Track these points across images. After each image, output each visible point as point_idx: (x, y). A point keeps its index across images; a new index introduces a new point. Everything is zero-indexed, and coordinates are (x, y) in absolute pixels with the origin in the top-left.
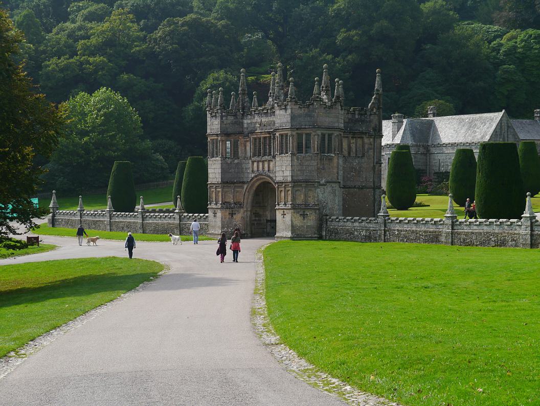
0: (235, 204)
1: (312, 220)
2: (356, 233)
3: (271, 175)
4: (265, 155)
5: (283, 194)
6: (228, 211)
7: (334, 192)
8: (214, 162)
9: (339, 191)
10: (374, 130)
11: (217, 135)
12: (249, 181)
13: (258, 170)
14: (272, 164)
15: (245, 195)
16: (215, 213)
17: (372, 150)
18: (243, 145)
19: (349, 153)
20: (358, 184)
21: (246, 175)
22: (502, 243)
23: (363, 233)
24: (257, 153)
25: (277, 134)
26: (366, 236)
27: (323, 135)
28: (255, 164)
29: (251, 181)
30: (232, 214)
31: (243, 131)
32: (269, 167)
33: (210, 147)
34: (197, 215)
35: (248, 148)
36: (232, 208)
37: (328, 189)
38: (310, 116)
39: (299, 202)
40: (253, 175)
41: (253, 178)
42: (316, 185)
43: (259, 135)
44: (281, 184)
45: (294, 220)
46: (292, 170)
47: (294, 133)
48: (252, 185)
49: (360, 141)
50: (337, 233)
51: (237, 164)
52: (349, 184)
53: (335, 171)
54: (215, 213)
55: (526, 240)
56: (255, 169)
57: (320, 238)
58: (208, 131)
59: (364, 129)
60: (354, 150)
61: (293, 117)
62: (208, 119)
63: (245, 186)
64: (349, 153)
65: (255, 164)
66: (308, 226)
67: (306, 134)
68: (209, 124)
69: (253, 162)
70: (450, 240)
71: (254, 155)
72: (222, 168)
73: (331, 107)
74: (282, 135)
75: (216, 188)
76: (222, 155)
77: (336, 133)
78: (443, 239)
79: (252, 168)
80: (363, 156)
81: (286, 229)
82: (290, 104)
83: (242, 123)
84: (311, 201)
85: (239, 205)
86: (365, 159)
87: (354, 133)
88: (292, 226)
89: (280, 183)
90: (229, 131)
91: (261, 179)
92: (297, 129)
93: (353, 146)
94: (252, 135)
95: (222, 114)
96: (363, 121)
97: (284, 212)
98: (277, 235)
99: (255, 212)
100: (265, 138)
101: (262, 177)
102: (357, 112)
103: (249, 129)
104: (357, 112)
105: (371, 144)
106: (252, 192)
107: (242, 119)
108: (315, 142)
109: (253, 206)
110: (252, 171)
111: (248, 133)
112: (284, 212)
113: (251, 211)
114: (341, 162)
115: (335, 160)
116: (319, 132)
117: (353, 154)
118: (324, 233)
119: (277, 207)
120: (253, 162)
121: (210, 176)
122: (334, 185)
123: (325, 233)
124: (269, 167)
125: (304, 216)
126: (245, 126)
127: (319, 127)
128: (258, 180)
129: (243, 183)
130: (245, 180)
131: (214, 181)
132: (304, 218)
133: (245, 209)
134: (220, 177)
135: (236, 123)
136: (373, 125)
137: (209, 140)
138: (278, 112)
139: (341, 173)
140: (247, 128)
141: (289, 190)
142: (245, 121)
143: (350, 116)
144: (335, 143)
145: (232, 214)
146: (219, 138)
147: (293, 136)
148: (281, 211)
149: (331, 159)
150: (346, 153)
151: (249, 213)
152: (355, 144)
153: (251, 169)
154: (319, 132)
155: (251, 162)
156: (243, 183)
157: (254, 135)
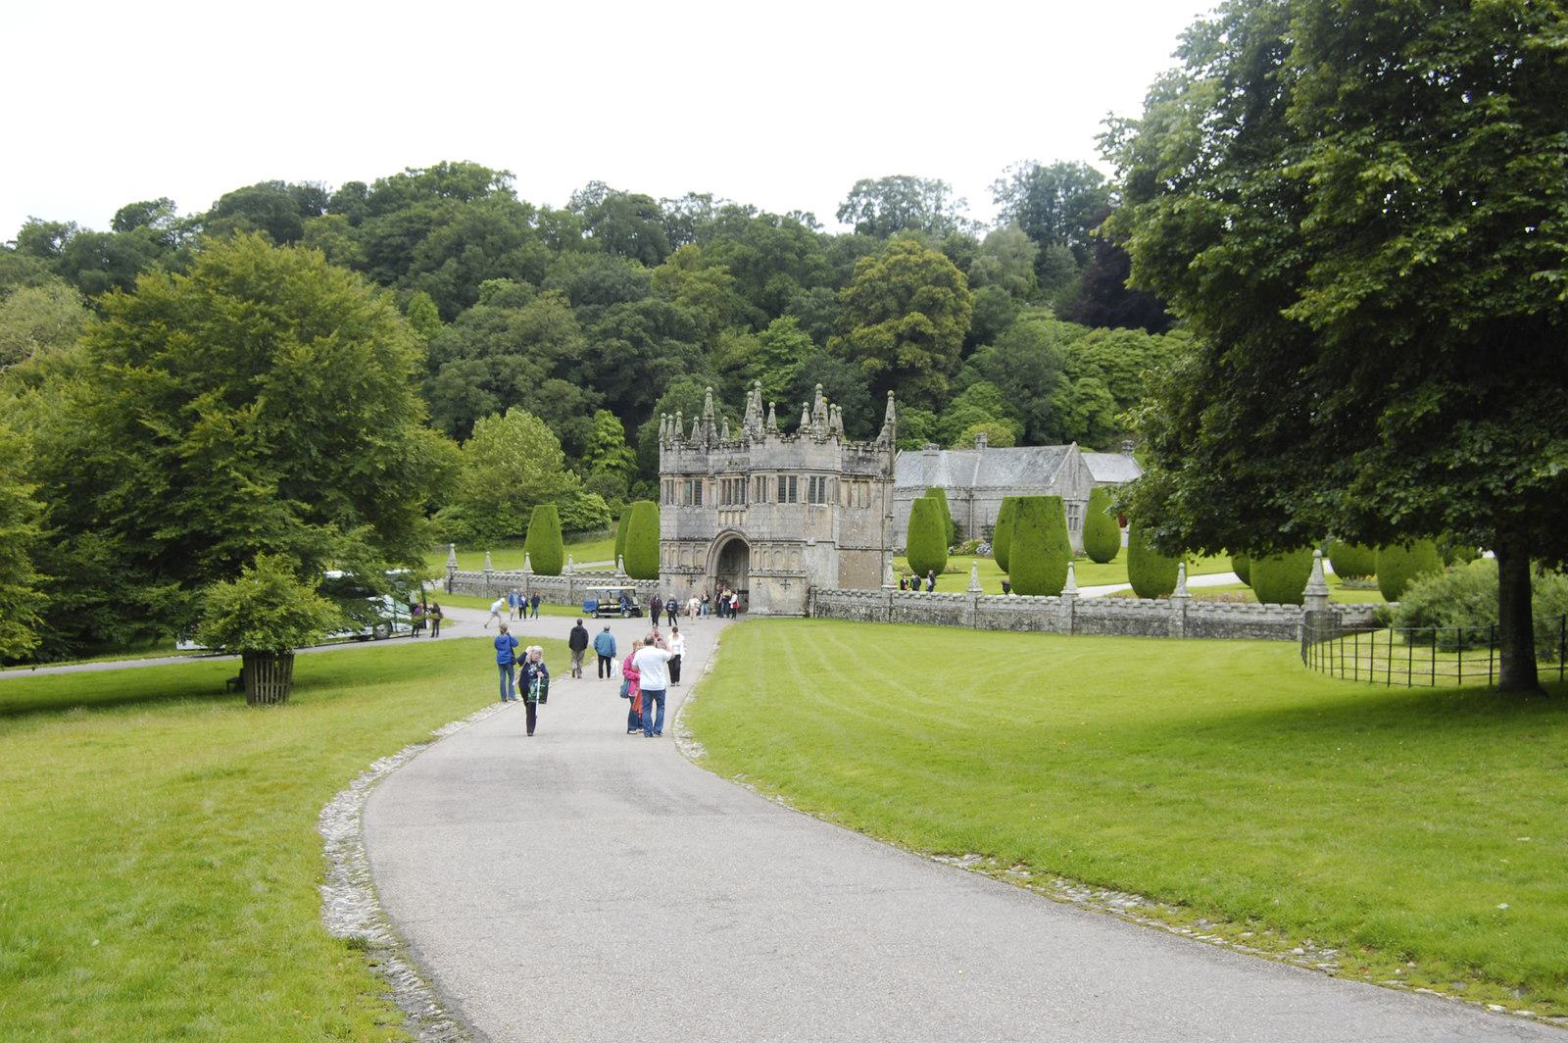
0: (695, 568)
1: (796, 592)
3: (744, 531)
4: (736, 503)
5: (758, 556)
6: (686, 578)
7: (826, 556)
9: (835, 556)
10: (884, 472)
11: (673, 475)
14: (744, 515)
15: (706, 558)
17: (880, 500)
19: (849, 503)
20: (861, 544)
22: (1035, 627)
23: (863, 611)
24: (726, 500)
25: (752, 476)
27: (813, 479)
32: (741, 520)
35: (714, 493)
37: (819, 550)
38: (796, 454)
39: (779, 567)
40: (720, 531)
42: (802, 545)
45: (772, 591)
48: (719, 543)
49: (864, 487)
51: (698, 515)
52: (848, 544)
53: (828, 527)
55: (1066, 624)
56: (723, 521)
57: (807, 615)
58: (662, 469)
59: (869, 471)
60: (856, 499)
62: (662, 453)
63: (709, 544)
64: (849, 503)
66: (790, 600)
67: (790, 477)
68: (662, 459)
69: (720, 512)
70: (973, 622)
73: (823, 442)
77: (830, 477)
78: (963, 620)
79: (718, 521)
80: (869, 506)
82: (768, 436)
83: (707, 460)
84: (795, 568)
86: (870, 512)
87: (856, 477)
90: (689, 470)
92: (778, 470)
93: (855, 494)
96: (869, 460)
98: (750, 610)
100: (737, 481)
102: (860, 448)
103: (716, 468)
104: (860, 448)
105: (879, 491)
106: (718, 552)
107: (707, 454)
108: (803, 487)
109: (719, 571)
113: (717, 578)
114: (836, 514)
115: (829, 513)
116: (808, 476)
117: (854, 504)
118: (811, 611)
119: (750, 574)
121: (663, 530)
122: (825, 545)
124: (741, 520)
125: (785, 586)
126: (711, 463)
127: (809, 470)
128: (726, 537)
129: (706, 540)
130: (709, 536)
131: (669, 537)
135: (697, 459)
136: (882, 466)
138: (753, 447)
139: (837, 530)
142: (711, 457)
143: (851, 453)
144: (829, 489)
148: (755, 580)
149: (822, 511)
150: (844, 502)
151: (714, 581)
152: (858, 490)
154: (808, 476)
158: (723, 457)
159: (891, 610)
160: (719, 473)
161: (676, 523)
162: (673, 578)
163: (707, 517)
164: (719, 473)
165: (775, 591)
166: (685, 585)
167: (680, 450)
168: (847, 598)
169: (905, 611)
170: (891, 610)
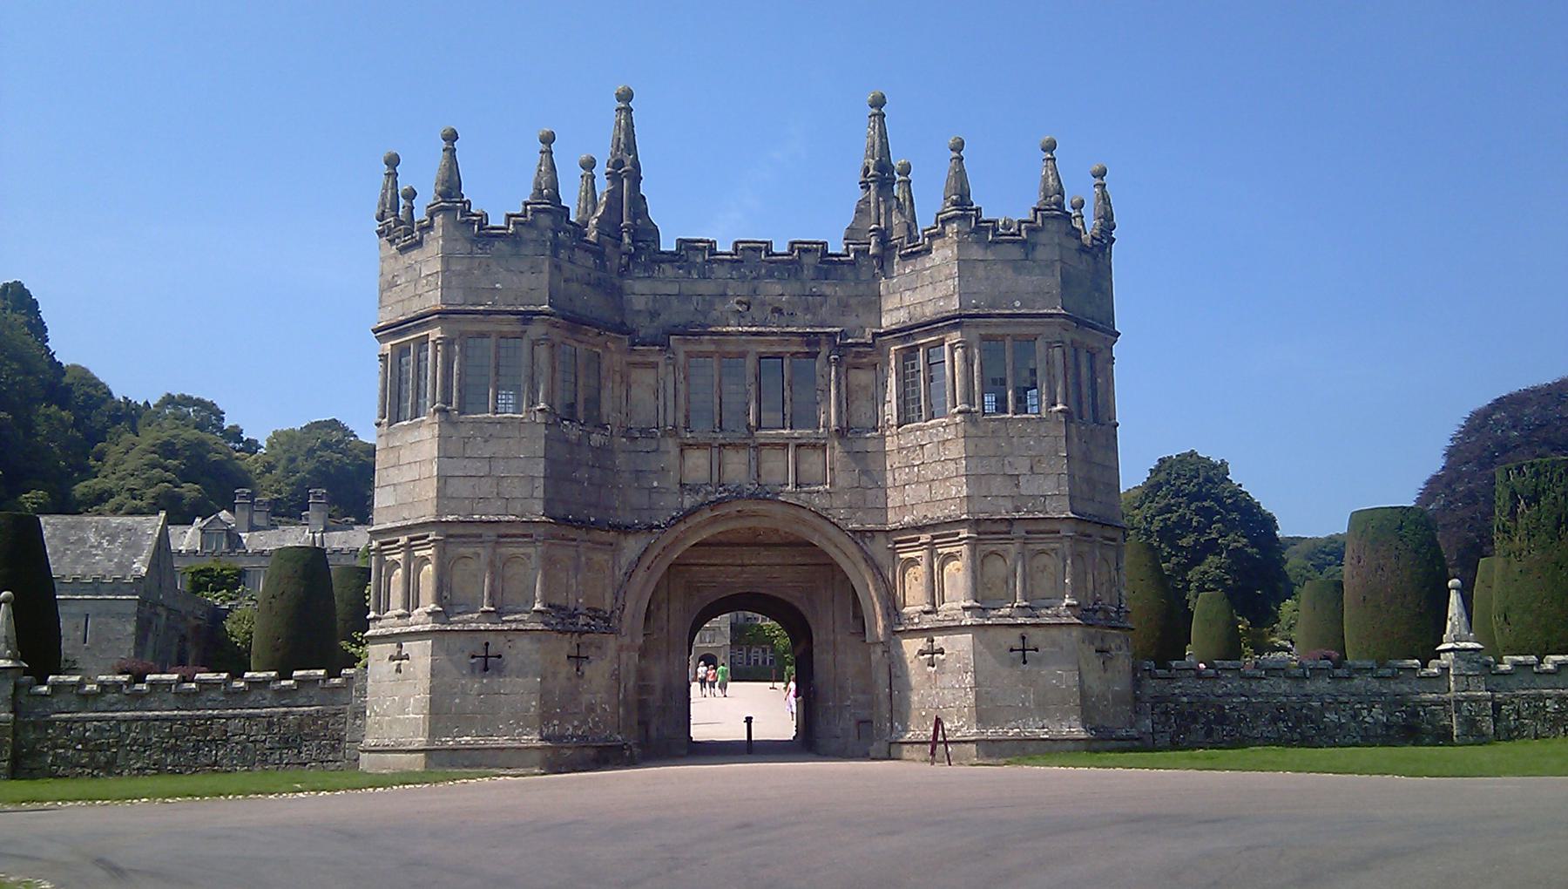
2: (1331, 717)
6: (566, 645)
8: (491, 430)
14: (812, 462)
18: (618, 378)
26: (1387, 726)
30: (577, 659)
36: (581, 633)
48: (675, 543)
50: (1222, 718)
63: (632, 546)
69: (684, 447)
85: (605, 622)
88: (1084, 696)
123: (1148, 722)
133: (627, 640)
134: (539, 493)
140: (654, 314)
145: (577, 659)
153: (673, 476)
155: (675, 451)
156: (626, 530)
158: (706, 287)
163: (620, 460)
166: (566, 669)
168: (1285, 686)
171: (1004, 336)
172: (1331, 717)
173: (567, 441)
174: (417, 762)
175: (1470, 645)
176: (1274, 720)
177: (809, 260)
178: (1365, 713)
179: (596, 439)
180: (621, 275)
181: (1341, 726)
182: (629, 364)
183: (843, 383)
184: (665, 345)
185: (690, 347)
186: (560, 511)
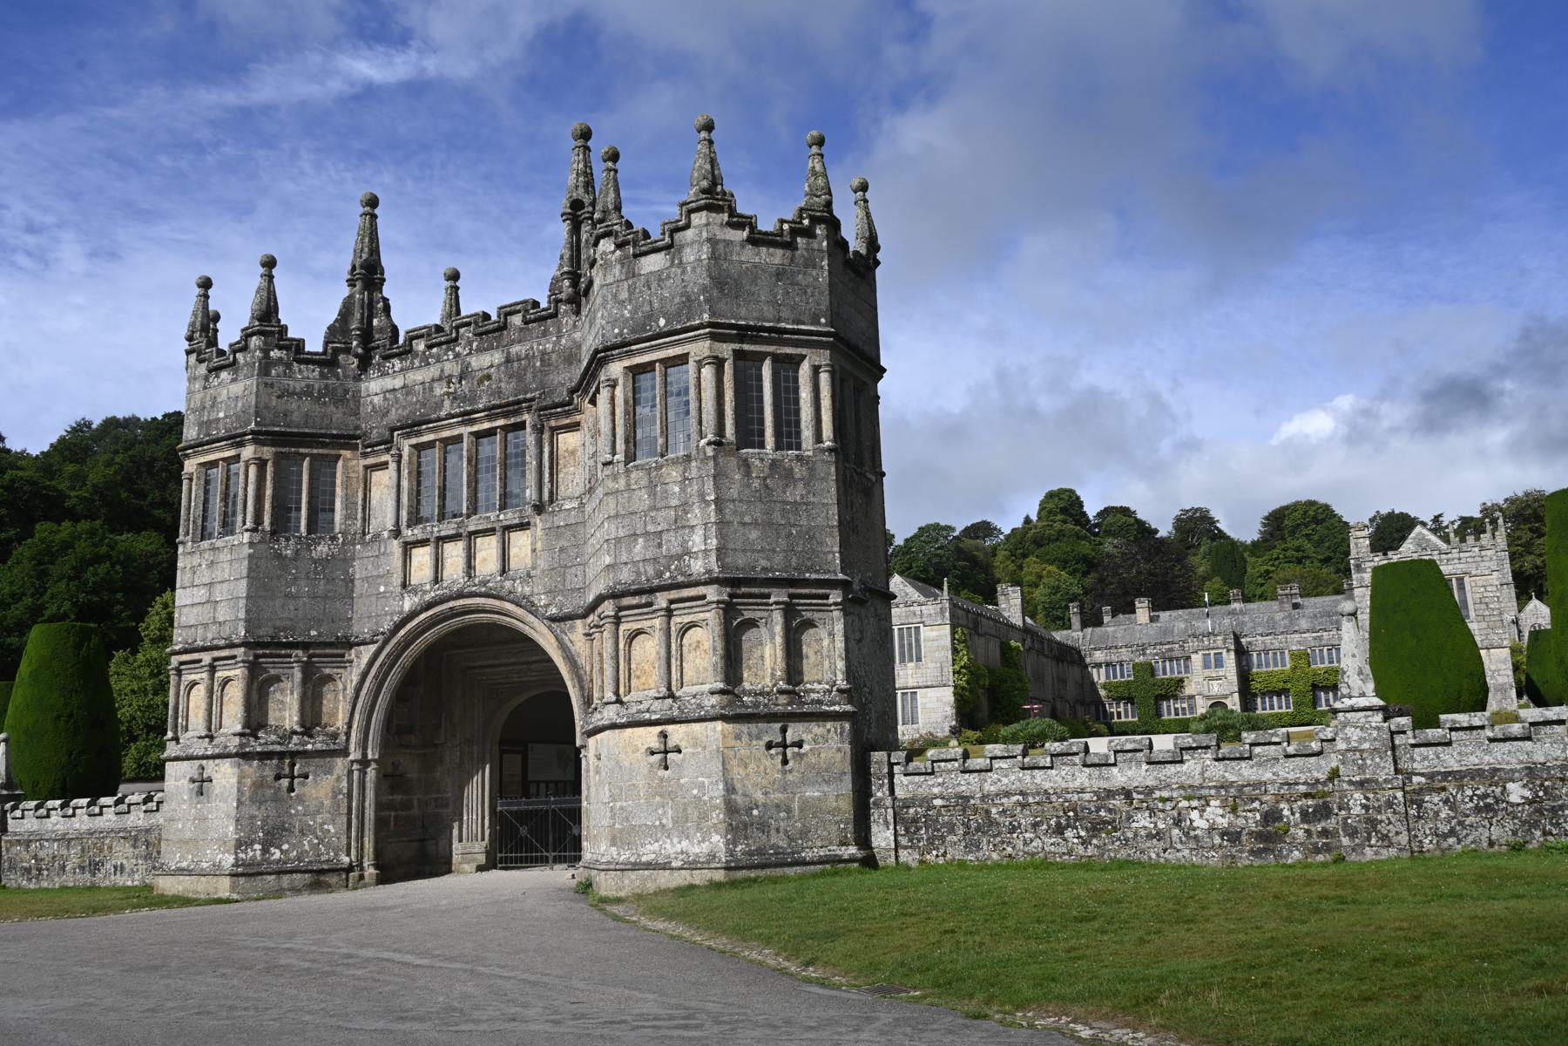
2: (1142, 821)
5: (648, 650)
12: (386, 626)
13: (437, 580)
14: (521, 544)
16: (201, 784)
21: (360, 607)
28: (422, 556)
29: (398, 626)
31: (357, 427)
33: (190, 496)
34: (84, 801)
40: (408, 604)
41: (413, 614)
43: (451, 426)
44: (644, 599)
45: (737, 772)
46: (722, 524)
47: (726, 350)
51: (325, 562)
54: (201, 784)
61: (723, 282)
65: (422, 556)
67: (777, 360)
69: (408, 547)
71: (416, 519)
72: (253, 575)
74: (636, 371)
75: (212, 669)
76: (258, 519)
81: (681, 826)
82: (698, 219)
83: (357, 396)
88: (731, 809)
89: (629, 598)
91: (454, 613)
94: (408, 436)
95: (266, 352)
97: (664, 735)
99: (390, 771)
101: (461, 602)
109: (385, 745)
110: (404, 585)
111: (393, 430)
112: (664, 735)
120: (408, 547)
123: (890, 834)
130: (362, 629)
132: (785, 762)
134: (242, 615)
135: (328, 391)
137: (190, 466)
141: (692, 625)
146: (248, 452)
147: (719, 363)
153: (397, 579)
157: (419, 434)
159: (1415, 798)
160: (411, 426)
161: (242, 588)
162: (225, 775)
163: (359, 570)
164: (411, 426)
165: (759, 773)
167: (266, 366)
169: (1517, 792)
170: (1415, 798)
171: (652, 363)
172: (1142, 821)
173: (279, 556)
174: (223, 887)
175: (1363, 702)
176: (1059, 830)
177: (517, 320)
178: (1195, 815)
179: (322, 549)
180: (357, 379)
181: (1159, 835)
182: (366, 467)
183: (546, 450)
184: (388, 442)
185: (414, 441)
186: (265, 632)
